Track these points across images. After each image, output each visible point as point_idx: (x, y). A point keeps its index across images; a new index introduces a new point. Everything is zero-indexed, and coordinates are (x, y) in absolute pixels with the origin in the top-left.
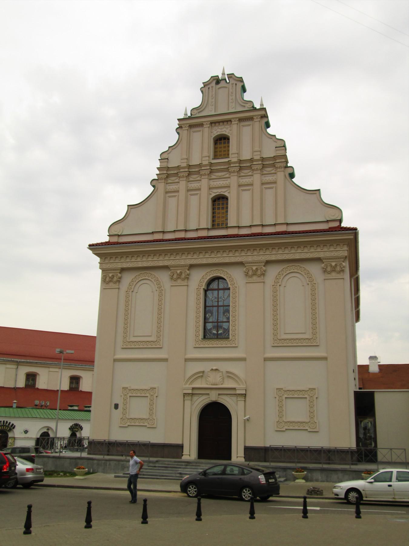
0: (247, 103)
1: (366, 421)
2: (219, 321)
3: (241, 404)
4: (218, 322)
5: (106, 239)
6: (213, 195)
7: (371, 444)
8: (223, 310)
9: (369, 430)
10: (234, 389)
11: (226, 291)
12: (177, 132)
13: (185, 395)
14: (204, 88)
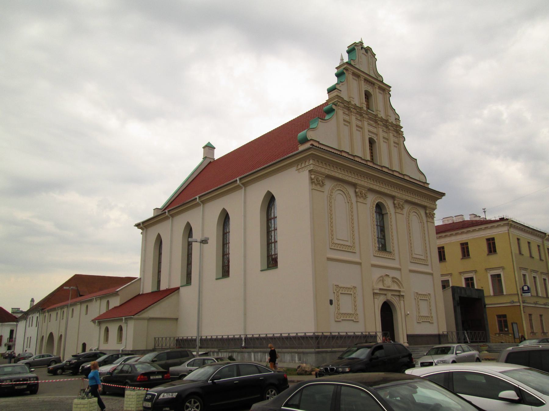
10: (399, 291)
13: (374, 294)
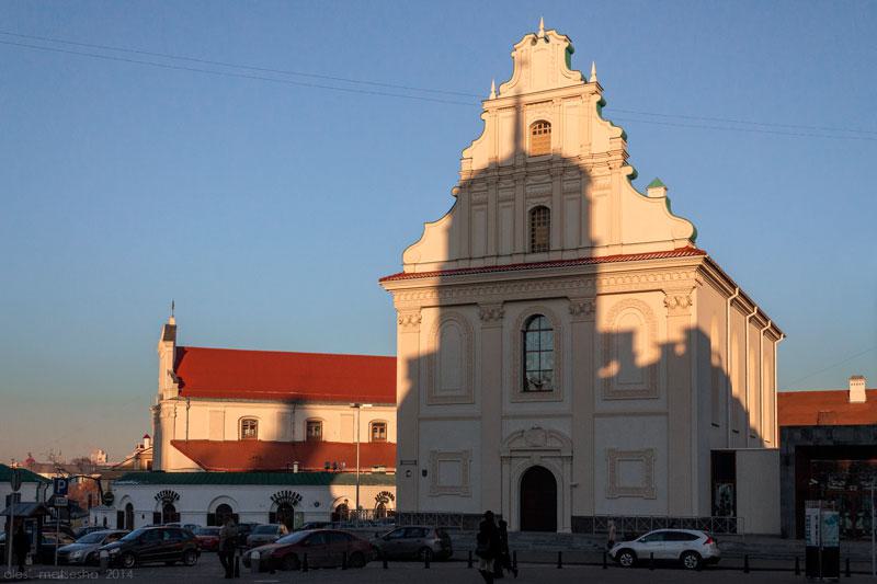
1: (725, 486)
3: (567, 467)
9: (727, 496)
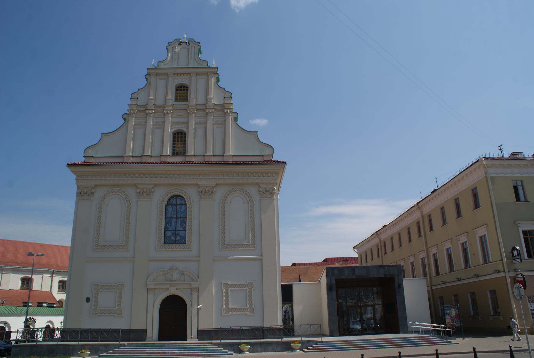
0: (203, 62)
2: (177, 230)
4: (176, 231)
5: (82, 160)
6: (174, 130)
7: (290, 322)
8: (180, 221)
9: (288, 312)
11: (183, 206)
12: (145, 78)
14: (169, 47)
